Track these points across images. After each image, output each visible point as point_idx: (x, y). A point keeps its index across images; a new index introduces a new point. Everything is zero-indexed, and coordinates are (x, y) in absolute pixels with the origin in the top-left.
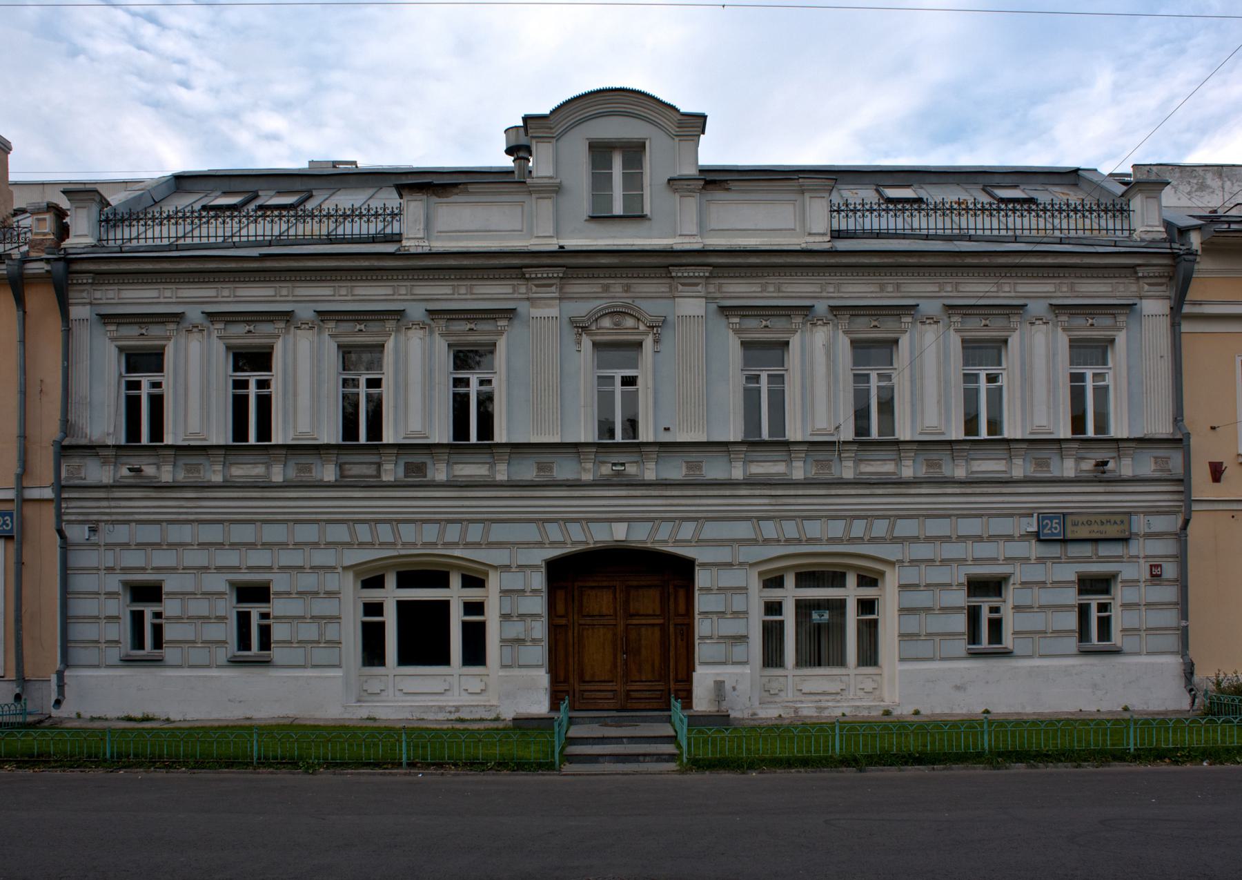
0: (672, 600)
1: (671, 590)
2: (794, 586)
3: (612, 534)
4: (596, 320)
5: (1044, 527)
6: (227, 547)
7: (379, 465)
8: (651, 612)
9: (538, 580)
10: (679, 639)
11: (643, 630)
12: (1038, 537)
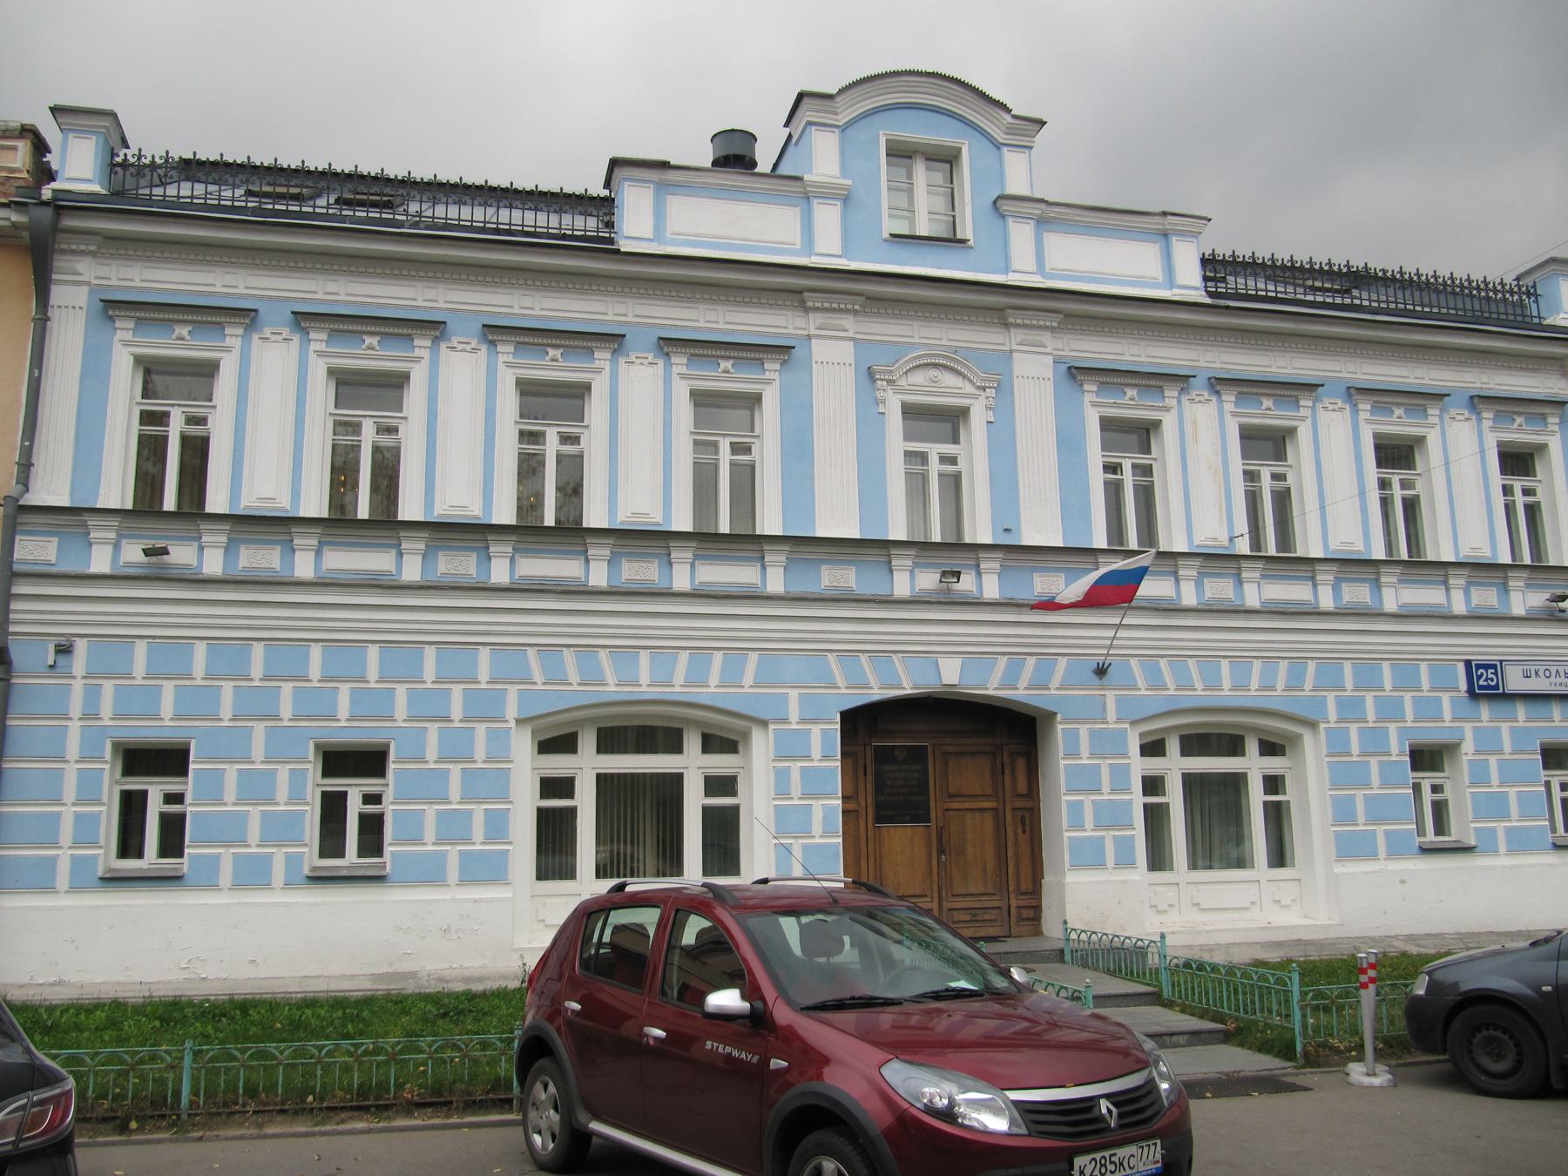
0: (1007, 771)
1: (1006, 759)
2: (1163, 758)
3: (941, 679)
4: (906, 373)
5: (1479, 677)
8: (979, 792)
10: (1020, 831)
11: (969, 816)
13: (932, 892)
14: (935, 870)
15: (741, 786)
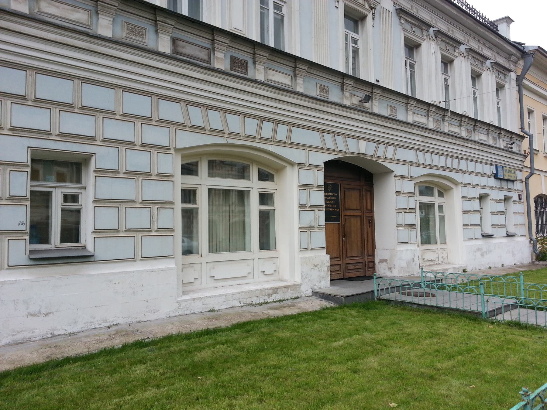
0: (364, 198)
6: (30, 103)
7: (211, 51)
9: (320, 178)
11: (352, 219)
12: (496, 176)
13: (340, 255)
14: (341, 245)
15: (276, 198)
